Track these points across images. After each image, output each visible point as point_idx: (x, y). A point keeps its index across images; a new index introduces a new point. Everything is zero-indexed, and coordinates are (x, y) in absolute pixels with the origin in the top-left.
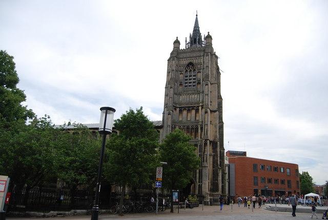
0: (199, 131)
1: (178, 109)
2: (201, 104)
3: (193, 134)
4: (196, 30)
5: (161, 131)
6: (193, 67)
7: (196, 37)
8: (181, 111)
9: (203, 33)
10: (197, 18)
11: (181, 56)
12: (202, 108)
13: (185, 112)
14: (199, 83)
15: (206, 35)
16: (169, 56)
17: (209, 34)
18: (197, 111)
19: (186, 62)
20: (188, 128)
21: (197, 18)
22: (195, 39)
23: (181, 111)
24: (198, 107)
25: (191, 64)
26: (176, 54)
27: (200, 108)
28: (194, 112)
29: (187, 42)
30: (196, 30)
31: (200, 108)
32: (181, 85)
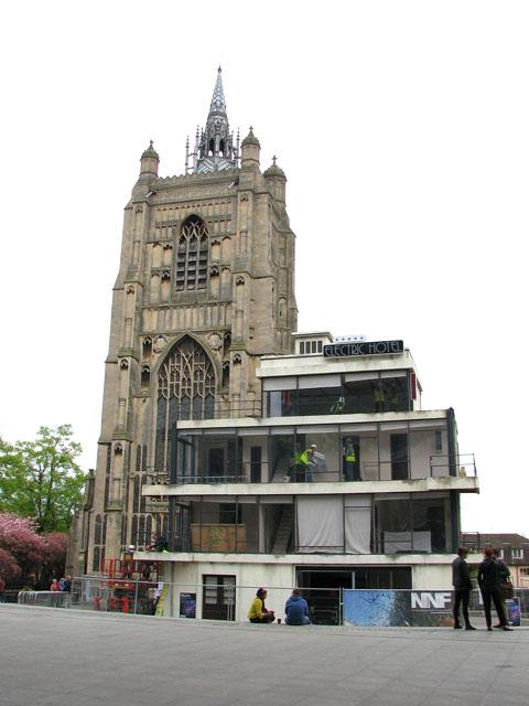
4: (217, 113)
7: (214, 140)
9: (238, 128)
10: (219, 79)
11: (163, 197)
15: (244, 135)
16: (127, 198)
17: (251, 134)
19: (181, 214)
21: (219, 79)
22: (212, 144)
25: (193, 221)
26: (151, 190)
29: (191, 150)
30: (217, 113)
32: (166, 279)
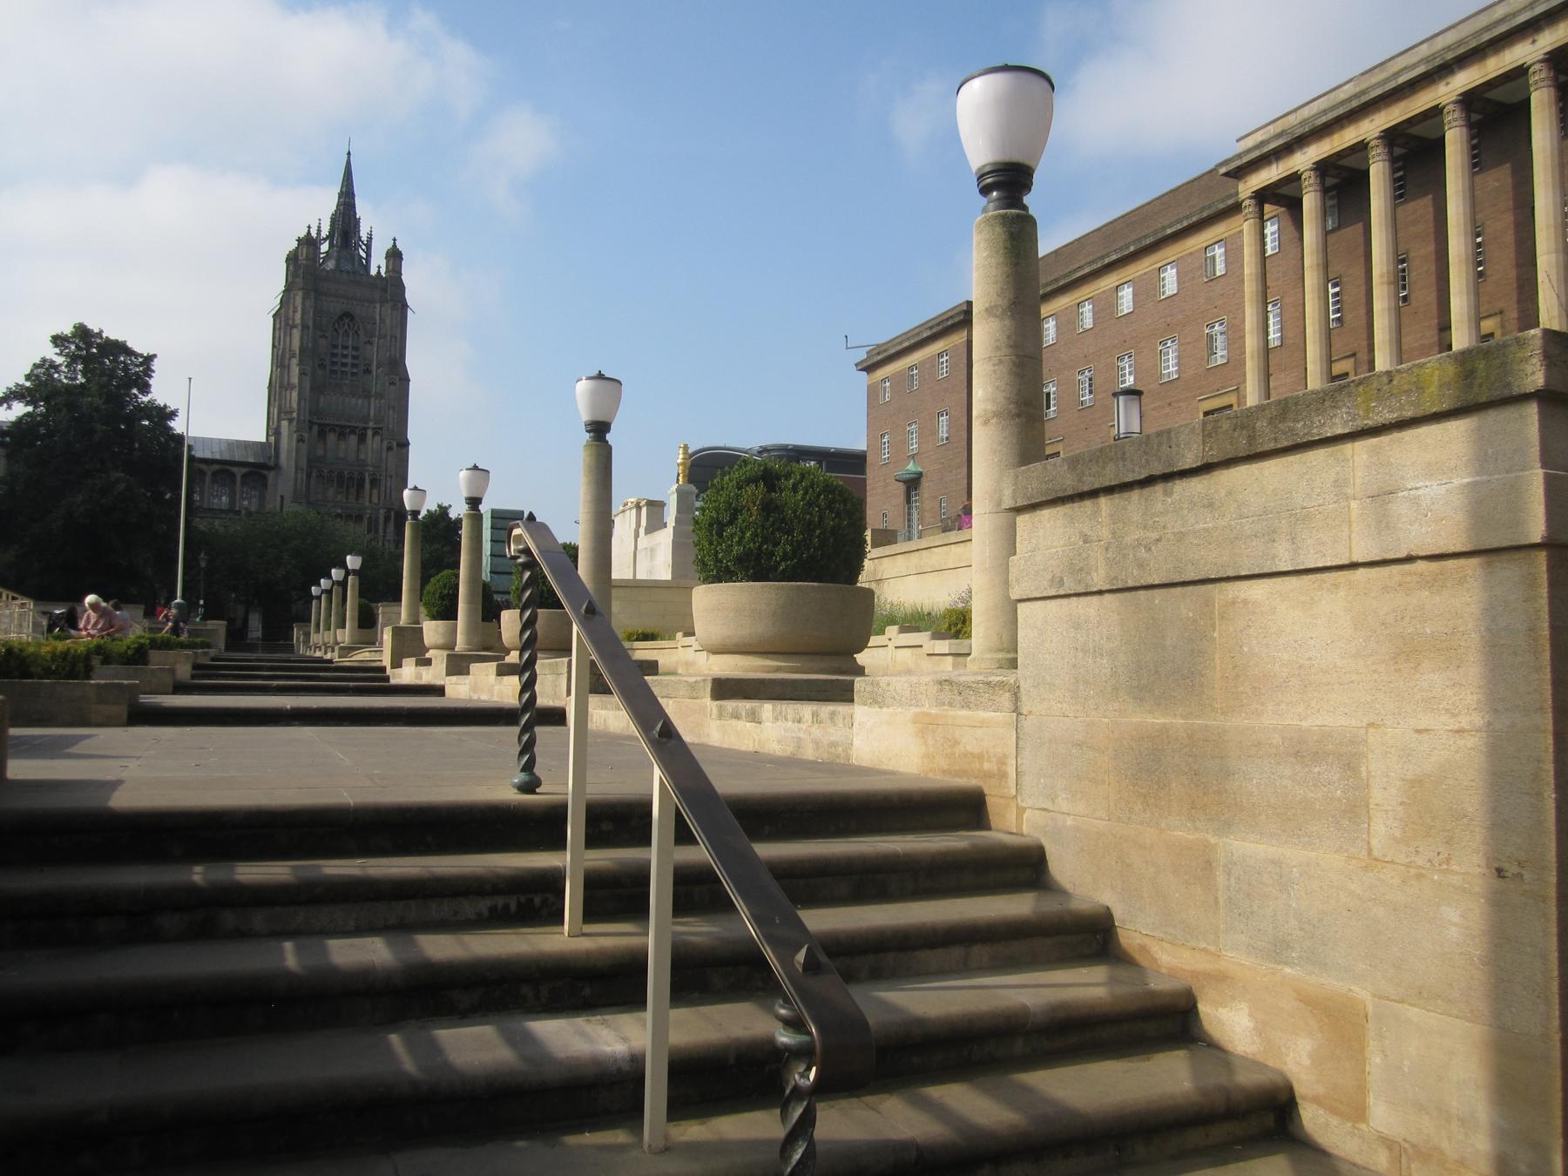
0: (367, 486)
1: (315, 428)
2: (371, 424)
3: (353, 490)
5: (271, 475)
6: (342, 314)
8: (322, 434)
9: (378, 226)
12: (374, 434)
13: (332, 438)
14: (368, 371)
18: (362, 438)
20: (341, 476)
23: (322, 434)
24: (365, 429)
25: (347, 315)
27: (370, 433)
28: (353, 439)
31: (370, 433)
32: (322, 366)
